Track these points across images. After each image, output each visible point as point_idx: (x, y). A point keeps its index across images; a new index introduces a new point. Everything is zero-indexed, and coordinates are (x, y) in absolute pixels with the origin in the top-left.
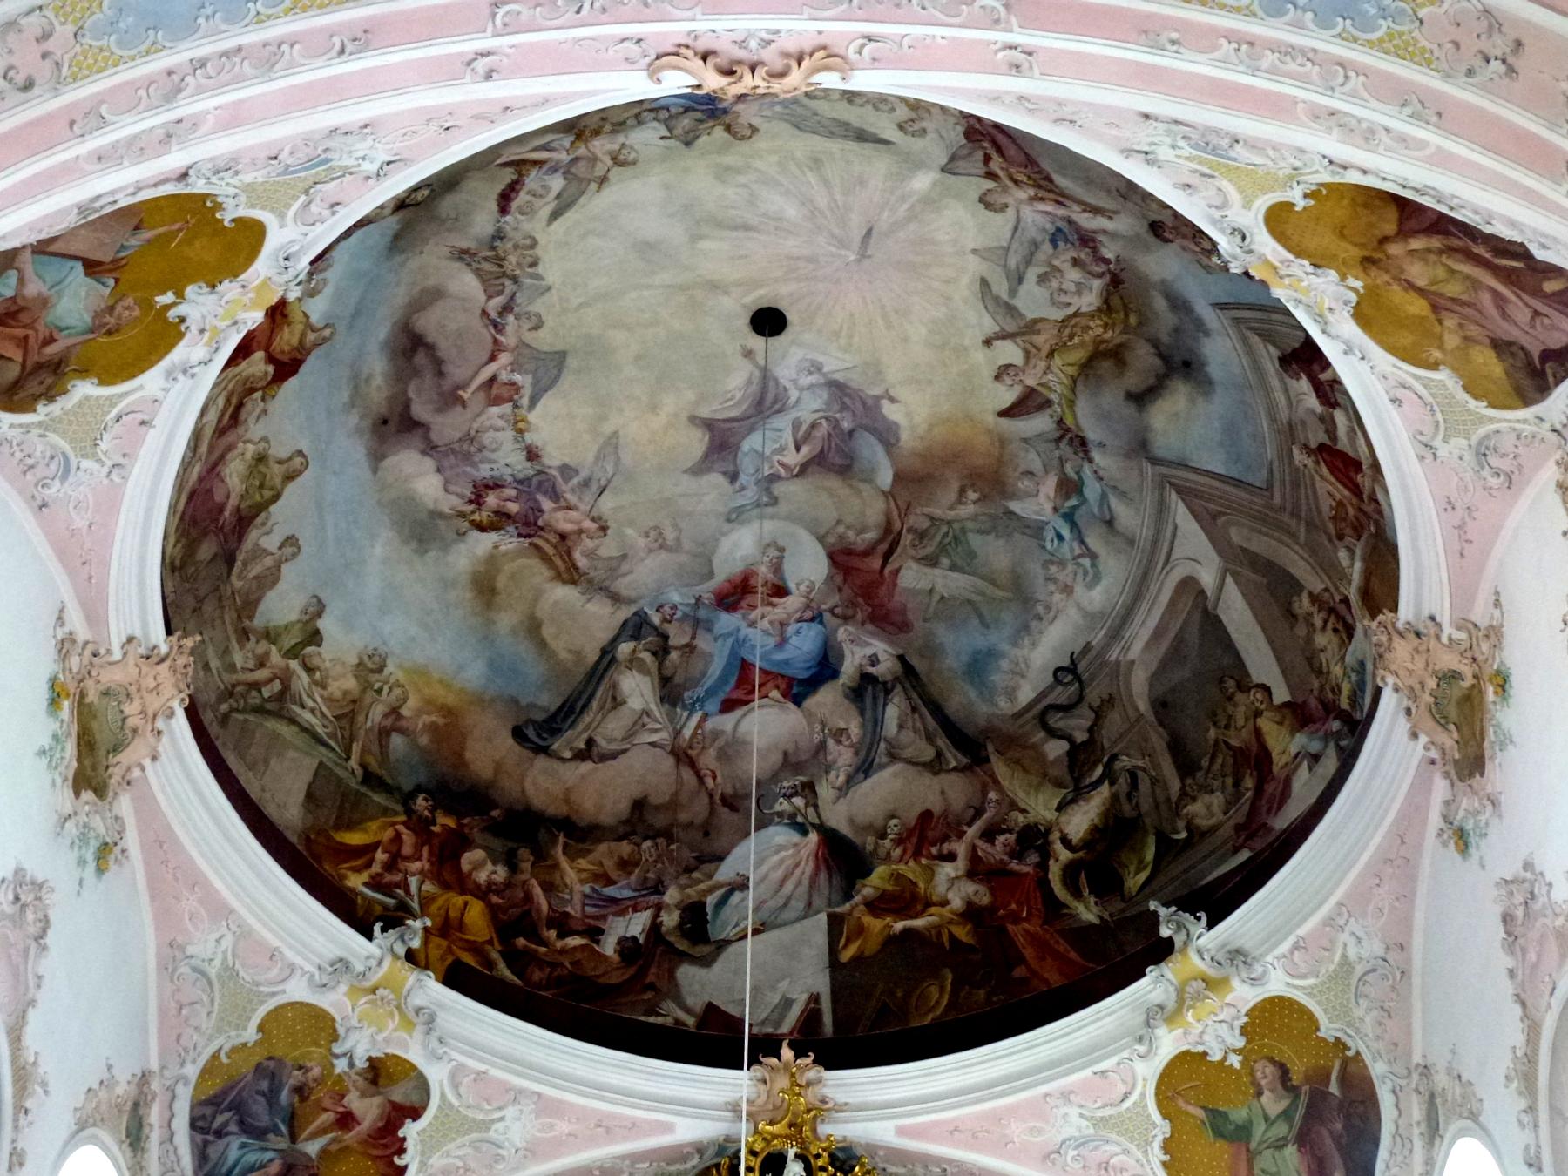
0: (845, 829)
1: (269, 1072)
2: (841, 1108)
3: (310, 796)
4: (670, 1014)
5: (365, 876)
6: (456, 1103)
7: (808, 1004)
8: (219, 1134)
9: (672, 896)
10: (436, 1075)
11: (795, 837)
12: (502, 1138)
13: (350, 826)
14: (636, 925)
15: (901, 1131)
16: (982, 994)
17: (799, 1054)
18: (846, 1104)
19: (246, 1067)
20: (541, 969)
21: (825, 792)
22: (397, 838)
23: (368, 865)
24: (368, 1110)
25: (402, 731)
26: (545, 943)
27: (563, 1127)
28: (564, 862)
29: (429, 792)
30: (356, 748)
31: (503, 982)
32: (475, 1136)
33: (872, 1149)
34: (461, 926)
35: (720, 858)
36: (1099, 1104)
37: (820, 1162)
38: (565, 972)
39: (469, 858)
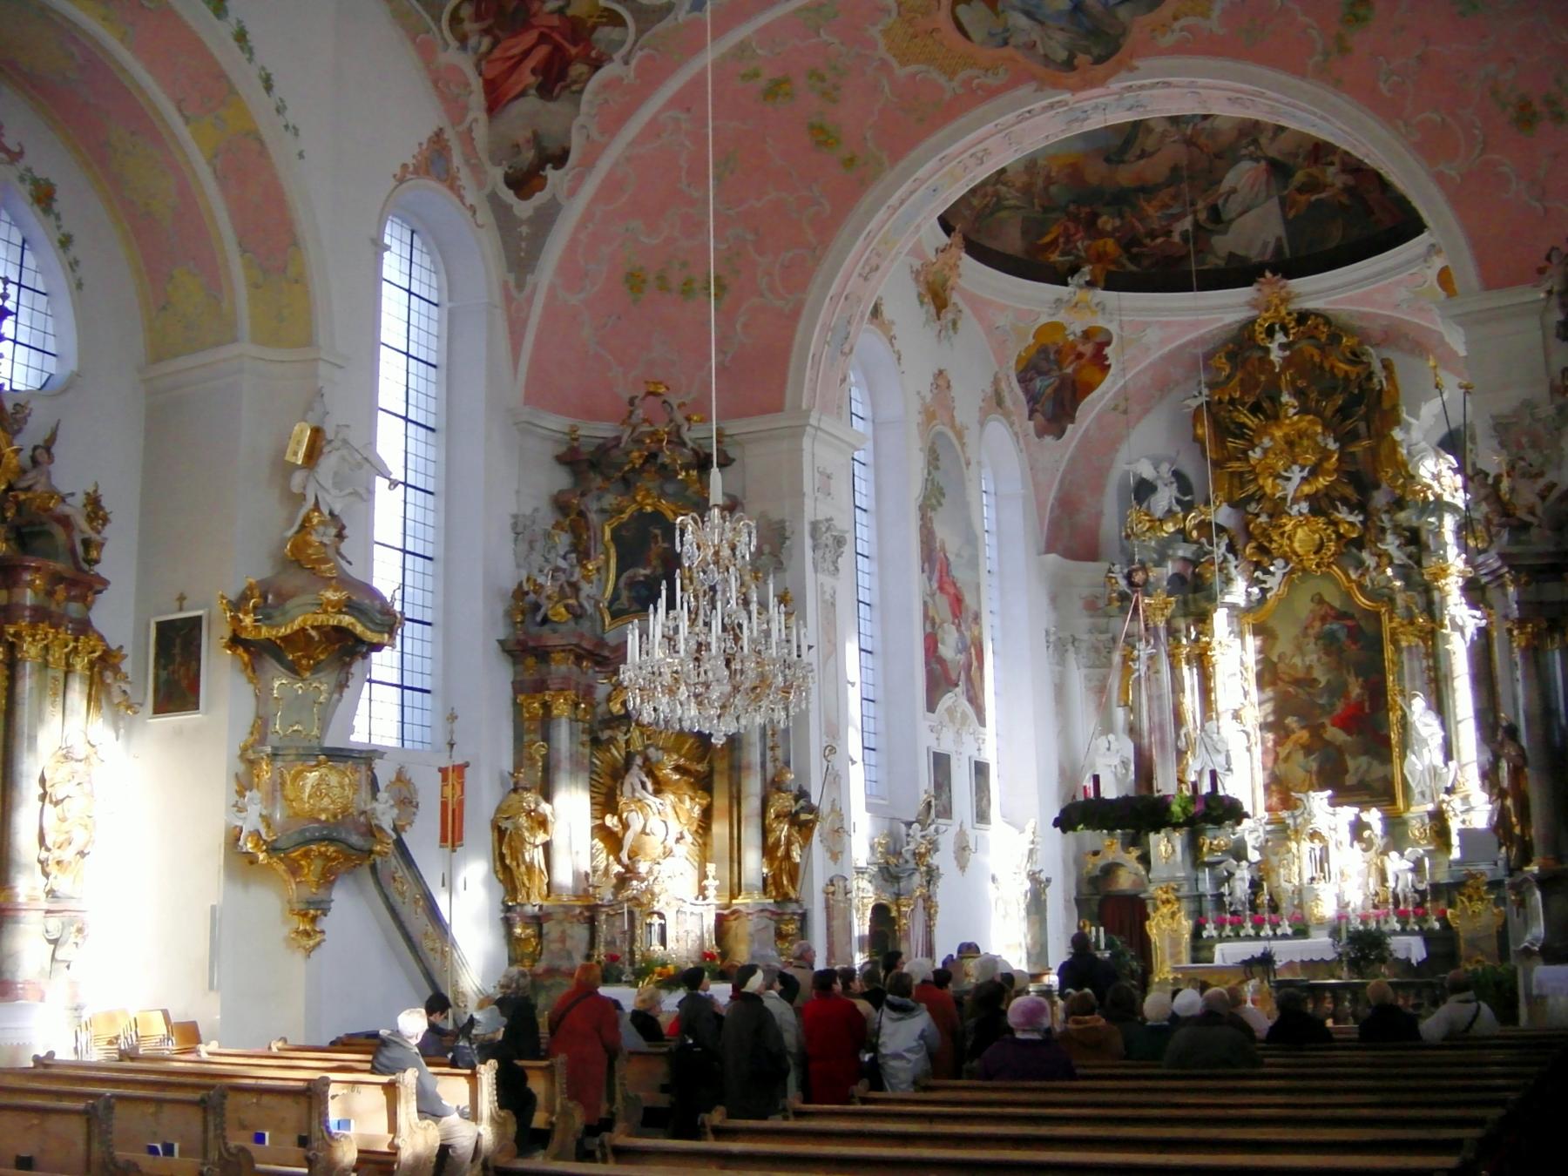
0: (1279, 158)
1: (1043, 351)
2: (1298, 295)
3: (1025, 233)
4: (1215, 261)
5: (1057, 252)
8: (1031, 380)
9: (1200, 205)
10: (1113, 328)
11: (1255, 164)
13: (1042, 235)
14: (1187, 224)
17: (1275, 274)
19: (1033, 351)
21: (1263, 141)
22: (1066, 229)
23: (1058, 246)
24: (1088, 349)
25: (1053, 184)
26: (1146, 246)
28: (1144, 204)
29: (1074, 202)
30: (1036, 201)
34: (1106, 253)
35: (1220, 182)
39: (1101, 221)
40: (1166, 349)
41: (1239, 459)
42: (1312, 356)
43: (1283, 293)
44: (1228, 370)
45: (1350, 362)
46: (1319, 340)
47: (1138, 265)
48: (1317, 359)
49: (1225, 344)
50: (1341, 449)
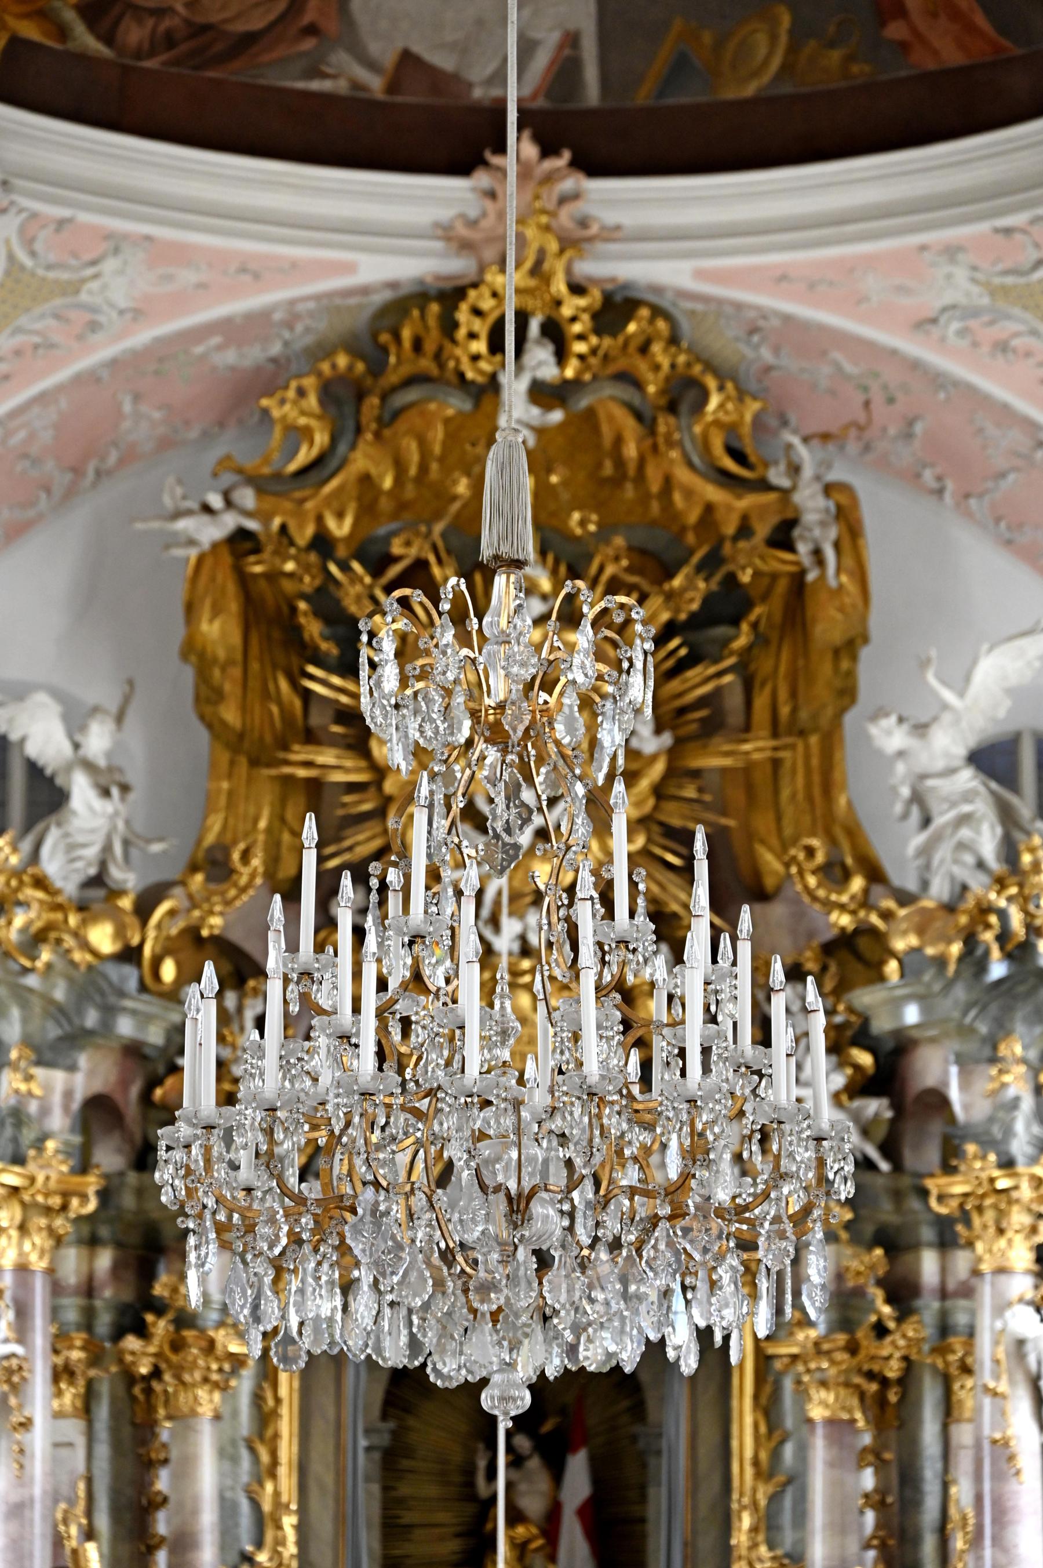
2: (612, 233)
6: (28, 262)
7: (561, 47)
12: (98, 300)
15: (700, 274)
16: (835, 56)
17: (548, 150)
18: (618, 228)
20: (140, 22)
27: (188, 277)
31: (83, 58)
32: (58, 302)
33: (658, 290)
36: (1000, 267)
37: (577, 328)
38: (176, 21)
40: (142, 337)
41: (333, 741)
42: (619, 441)
43: (565, 217)
44: (321, 439)
45: (725, 478)
46: (638, 385)
47: (108, 40)
48: (631, 451)
49: (323, 351)
50: (673, 753)
